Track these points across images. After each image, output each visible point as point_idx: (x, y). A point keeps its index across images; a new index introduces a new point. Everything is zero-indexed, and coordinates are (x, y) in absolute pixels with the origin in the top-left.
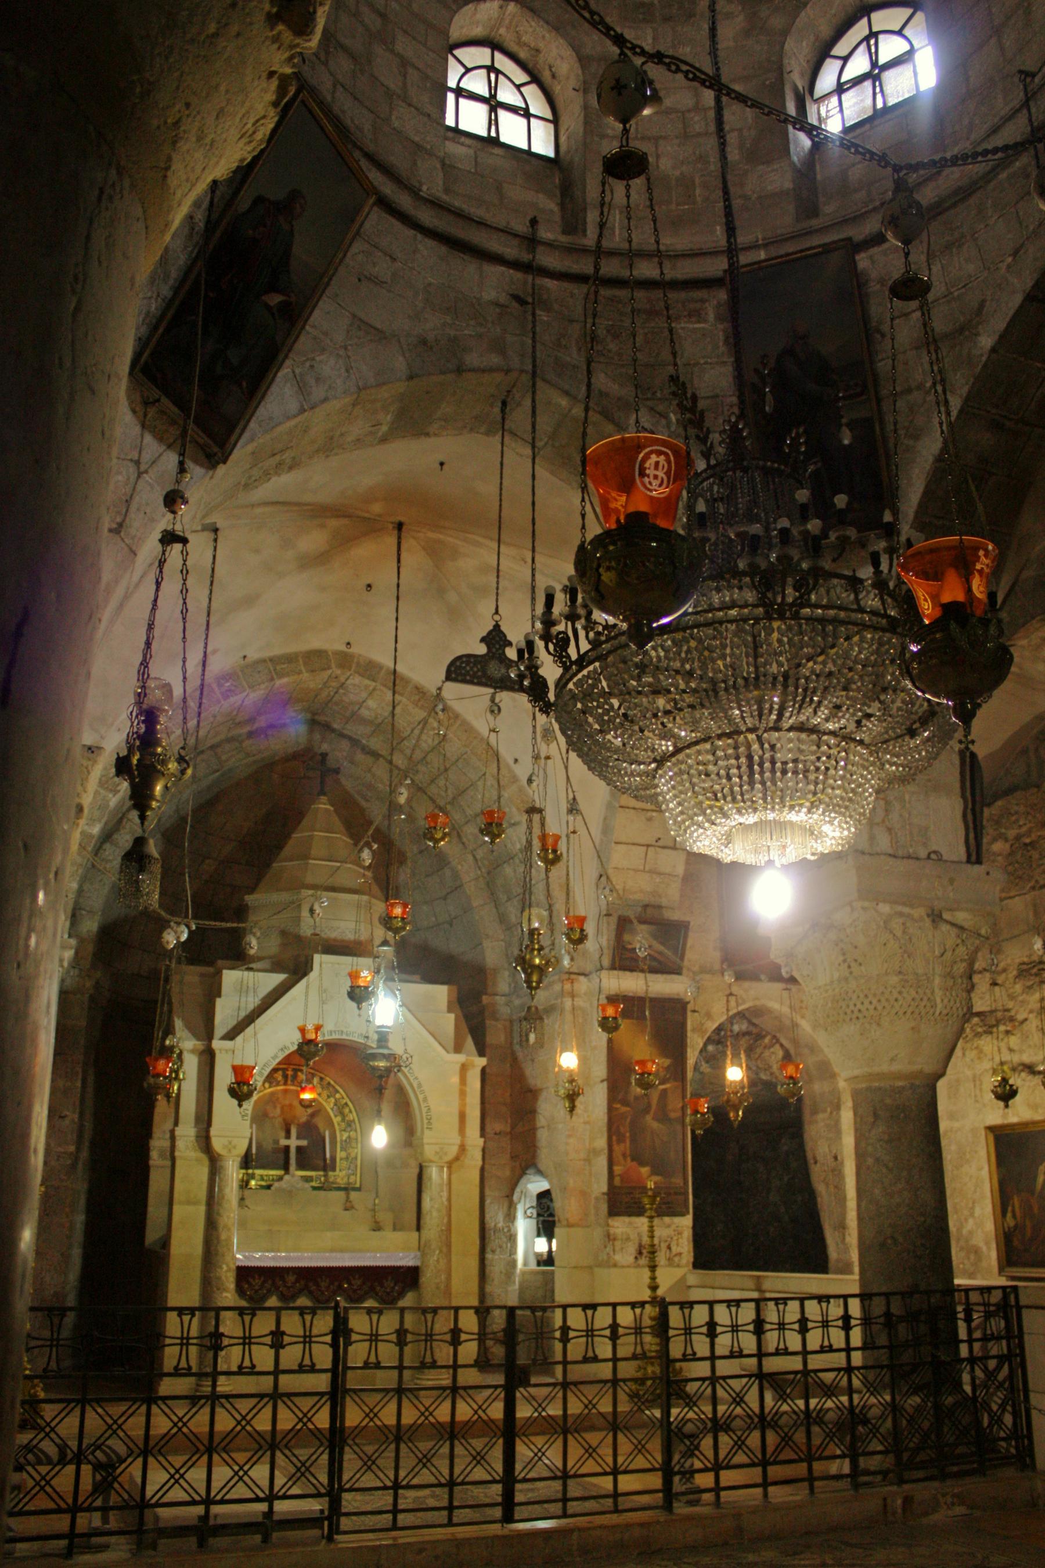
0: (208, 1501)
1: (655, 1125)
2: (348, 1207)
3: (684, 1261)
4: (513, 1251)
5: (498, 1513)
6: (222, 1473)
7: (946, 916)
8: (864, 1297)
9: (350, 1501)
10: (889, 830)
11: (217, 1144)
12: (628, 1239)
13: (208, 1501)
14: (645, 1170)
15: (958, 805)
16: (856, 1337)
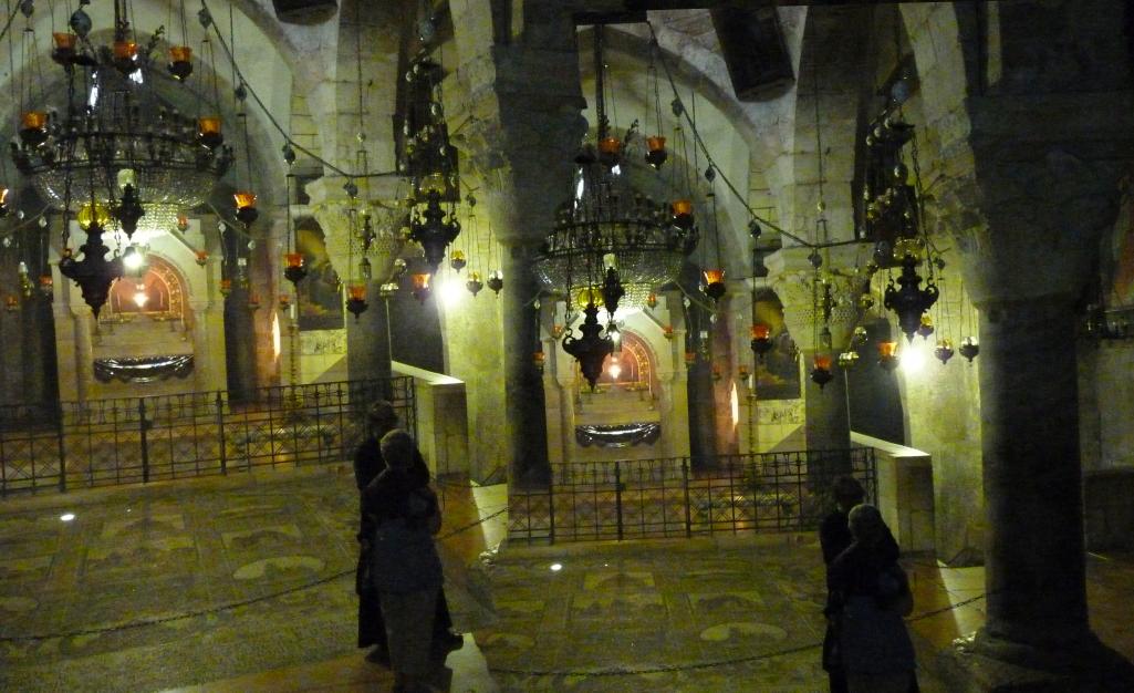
0: (529, 530)
1: (780, 354)
2: (642, 400)
3: (800, 420)
4: (730, 414)
5: (616, 536)
6: (534, 521)
7: (841, 271)
8: (808, 452)
9: (557, 532)
10: (807, 232)
11: (560, 381)
12: (768, 411)
13: (529, 530)
14: (775, 377)
15: (852, 212)
16: (804, 470)
